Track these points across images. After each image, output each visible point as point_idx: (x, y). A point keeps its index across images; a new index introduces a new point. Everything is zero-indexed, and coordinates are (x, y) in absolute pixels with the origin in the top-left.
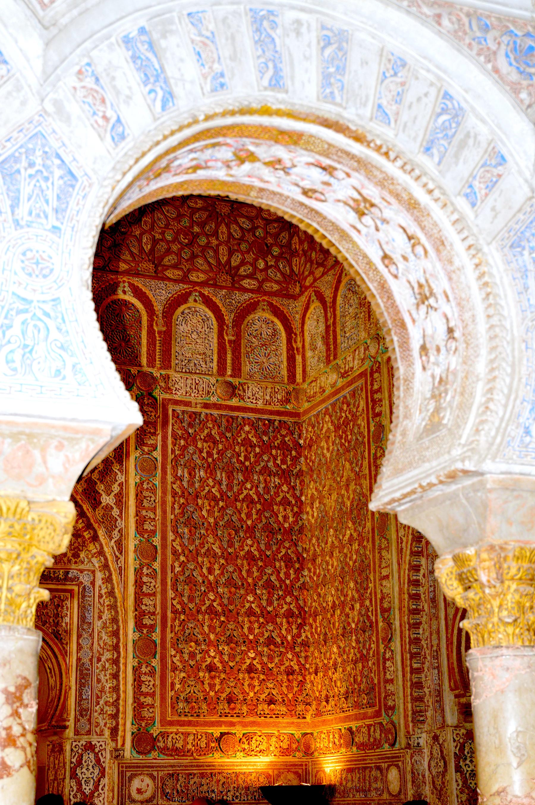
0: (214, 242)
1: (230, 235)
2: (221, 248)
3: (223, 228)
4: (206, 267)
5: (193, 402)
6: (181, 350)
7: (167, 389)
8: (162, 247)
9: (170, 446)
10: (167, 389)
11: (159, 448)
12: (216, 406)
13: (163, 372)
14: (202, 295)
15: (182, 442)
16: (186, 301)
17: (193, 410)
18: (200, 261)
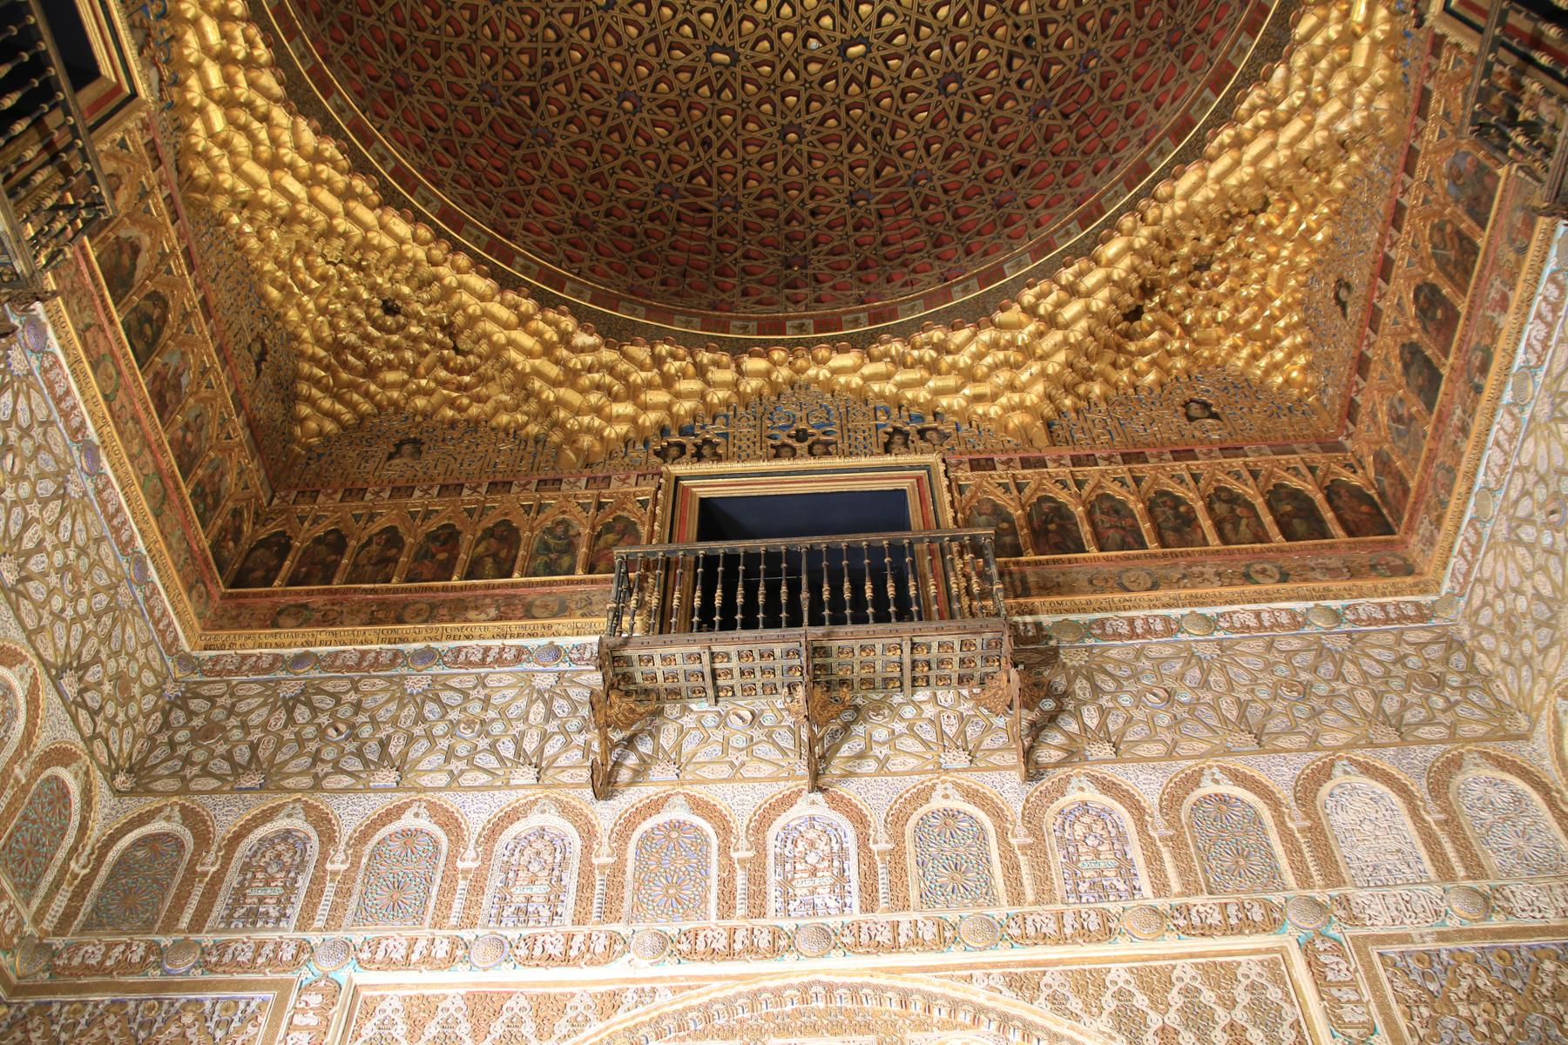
0: (1342, 688)
1: (1365, 674)
2: (1357, 694)
3: (1348, 668)
4: (1343, 722)
5: (1415, 933)
6: (1354, 851)
7: (1353, 919)
8: (1255, 712)
9: (1402, 1023)
10: (1353, 919)
11: (1380, 1027)
12: (1461, 934)
13: (1334, 893)
14: (1352, 762)
15: (1425, 1012)
16: (1329, 777)
17: (1421, 947)
18: (1330, 715)
